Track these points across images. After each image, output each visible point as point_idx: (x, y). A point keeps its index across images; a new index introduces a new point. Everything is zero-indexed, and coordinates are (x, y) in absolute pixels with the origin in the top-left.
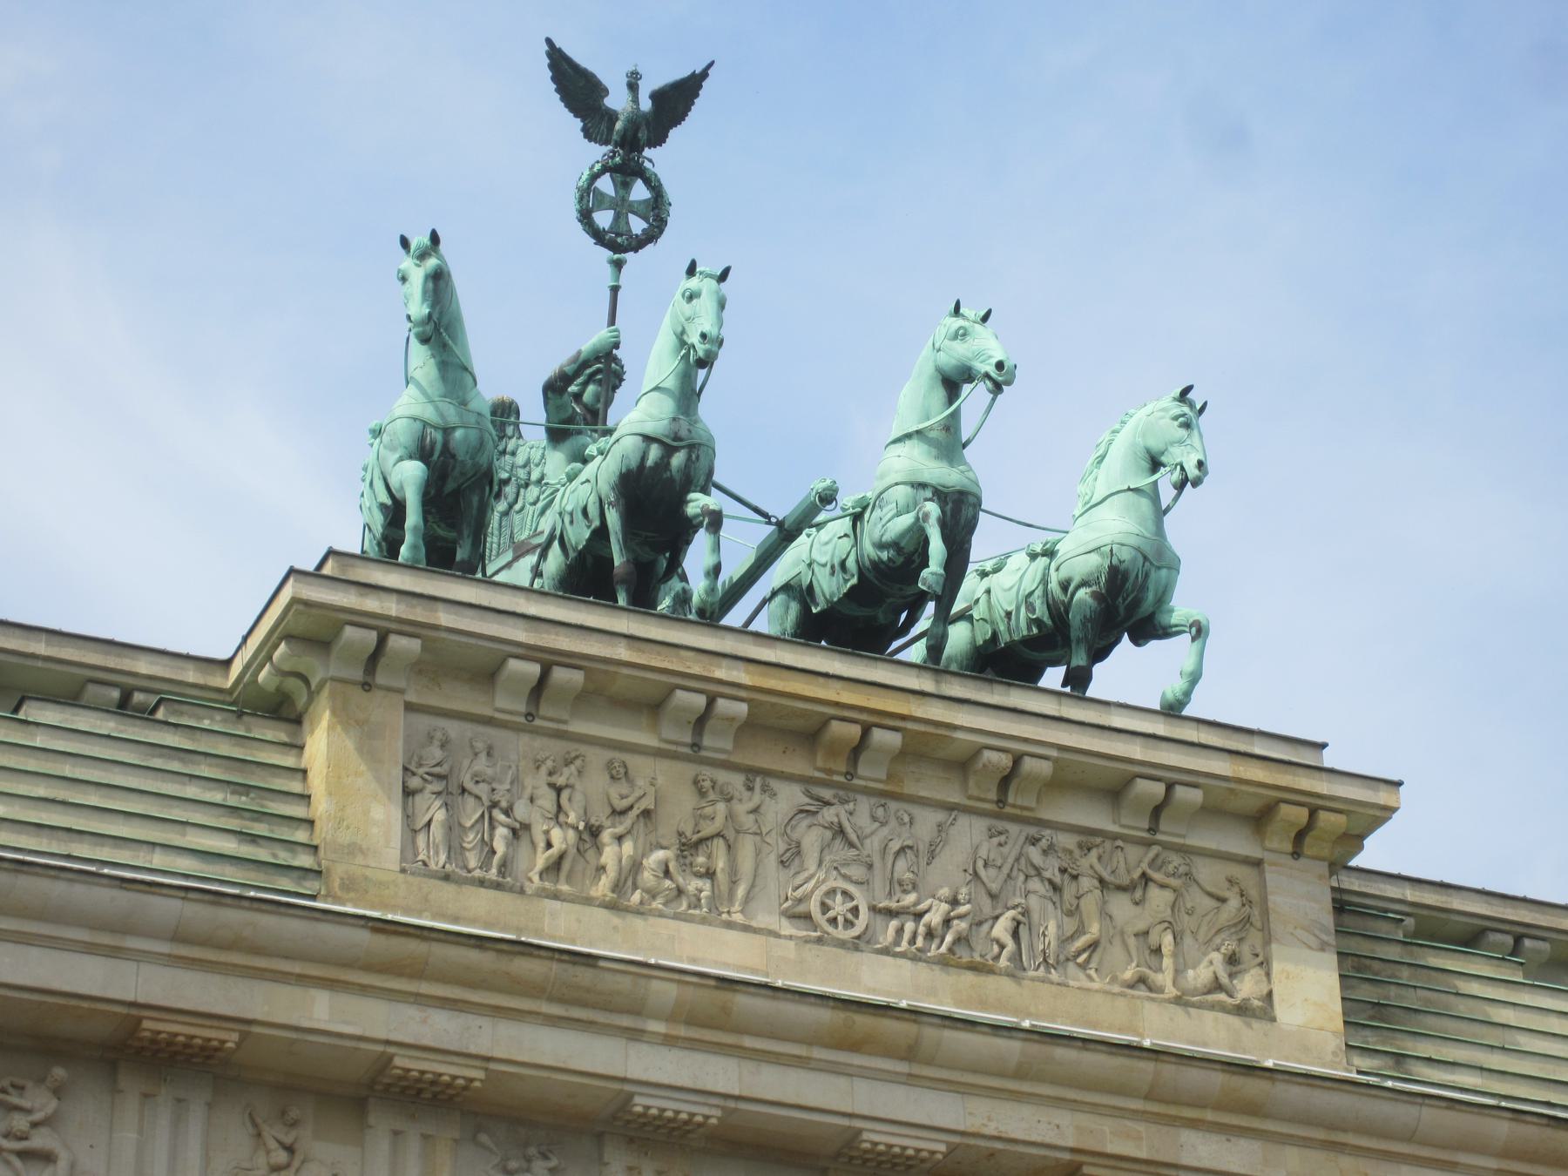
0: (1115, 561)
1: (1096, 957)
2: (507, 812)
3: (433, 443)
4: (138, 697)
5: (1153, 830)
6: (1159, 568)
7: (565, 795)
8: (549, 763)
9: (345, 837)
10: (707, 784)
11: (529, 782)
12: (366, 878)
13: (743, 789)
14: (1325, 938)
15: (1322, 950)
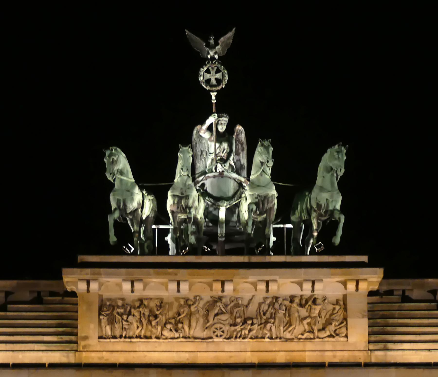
0: (318, 202)
1: (295, 331)
2: (127, 321)
3: (120, 203)
4: (42, 294)
5: (313, 290)
6: (332, 201)
7: (142, 312)
8: (137, 304)
9: (83, 335)
10: (182, 302)
11: (133, 310)
12: (89, 345)
13: (193, 300)
14: (364, 314)
15: (363, 317)
